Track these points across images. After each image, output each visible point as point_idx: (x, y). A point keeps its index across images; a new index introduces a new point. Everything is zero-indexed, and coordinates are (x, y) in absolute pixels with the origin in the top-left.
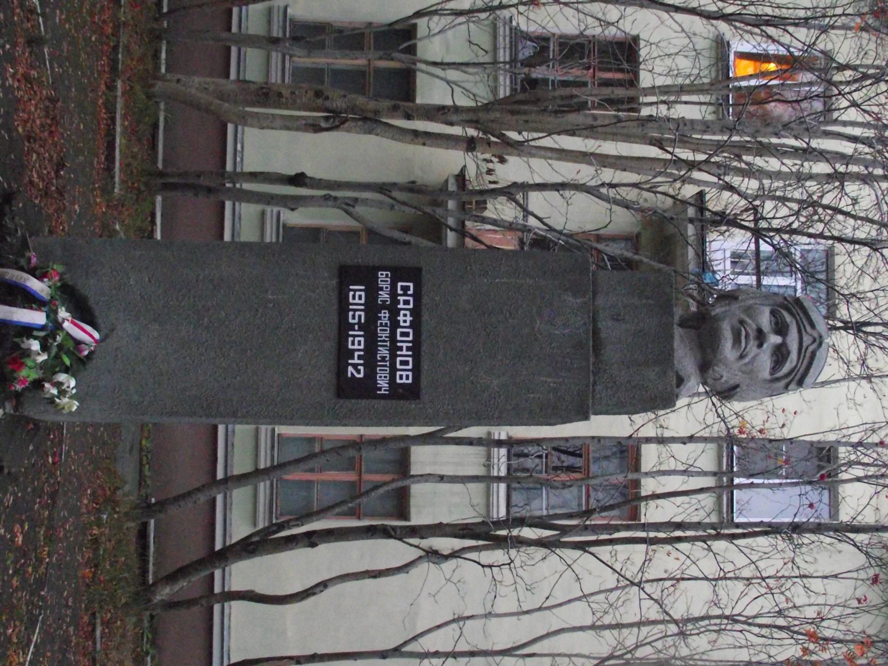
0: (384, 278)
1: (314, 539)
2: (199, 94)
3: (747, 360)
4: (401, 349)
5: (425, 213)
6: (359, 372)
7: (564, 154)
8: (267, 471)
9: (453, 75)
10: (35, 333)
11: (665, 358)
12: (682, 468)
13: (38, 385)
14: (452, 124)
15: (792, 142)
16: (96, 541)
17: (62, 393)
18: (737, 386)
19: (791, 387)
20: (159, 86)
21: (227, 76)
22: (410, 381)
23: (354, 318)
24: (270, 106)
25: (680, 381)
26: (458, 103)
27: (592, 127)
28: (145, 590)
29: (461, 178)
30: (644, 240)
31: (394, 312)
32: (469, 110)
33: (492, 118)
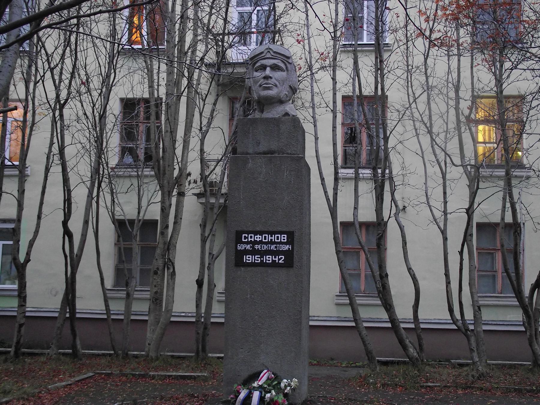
0: (240, 247)
1: (384, 275)
2: (156, 333)
3: (277, 83)
4: (271, 240)
6: (282, 258)
7: (186, 143)
8: (350, 299)
9: (144, 203)
10: (263, 396)
11: (276, 122)
13: (286, 395)
15: (177, 26)
16: (383, 385)
17: (289, 385)
18: (290, 86)
19: (290, 61)
20: (152, 354)
21: (147, 321)
22: (286, 236)
23: (258, 260)
24: (162, 298)
25: (287, 114)
26: (160, 199)
27: (171, 132)
28: (413, 362)
29: (199, 196)
30: (232, 95)
31: (255, 242)
32: (163, 194)
33: (167, 184)
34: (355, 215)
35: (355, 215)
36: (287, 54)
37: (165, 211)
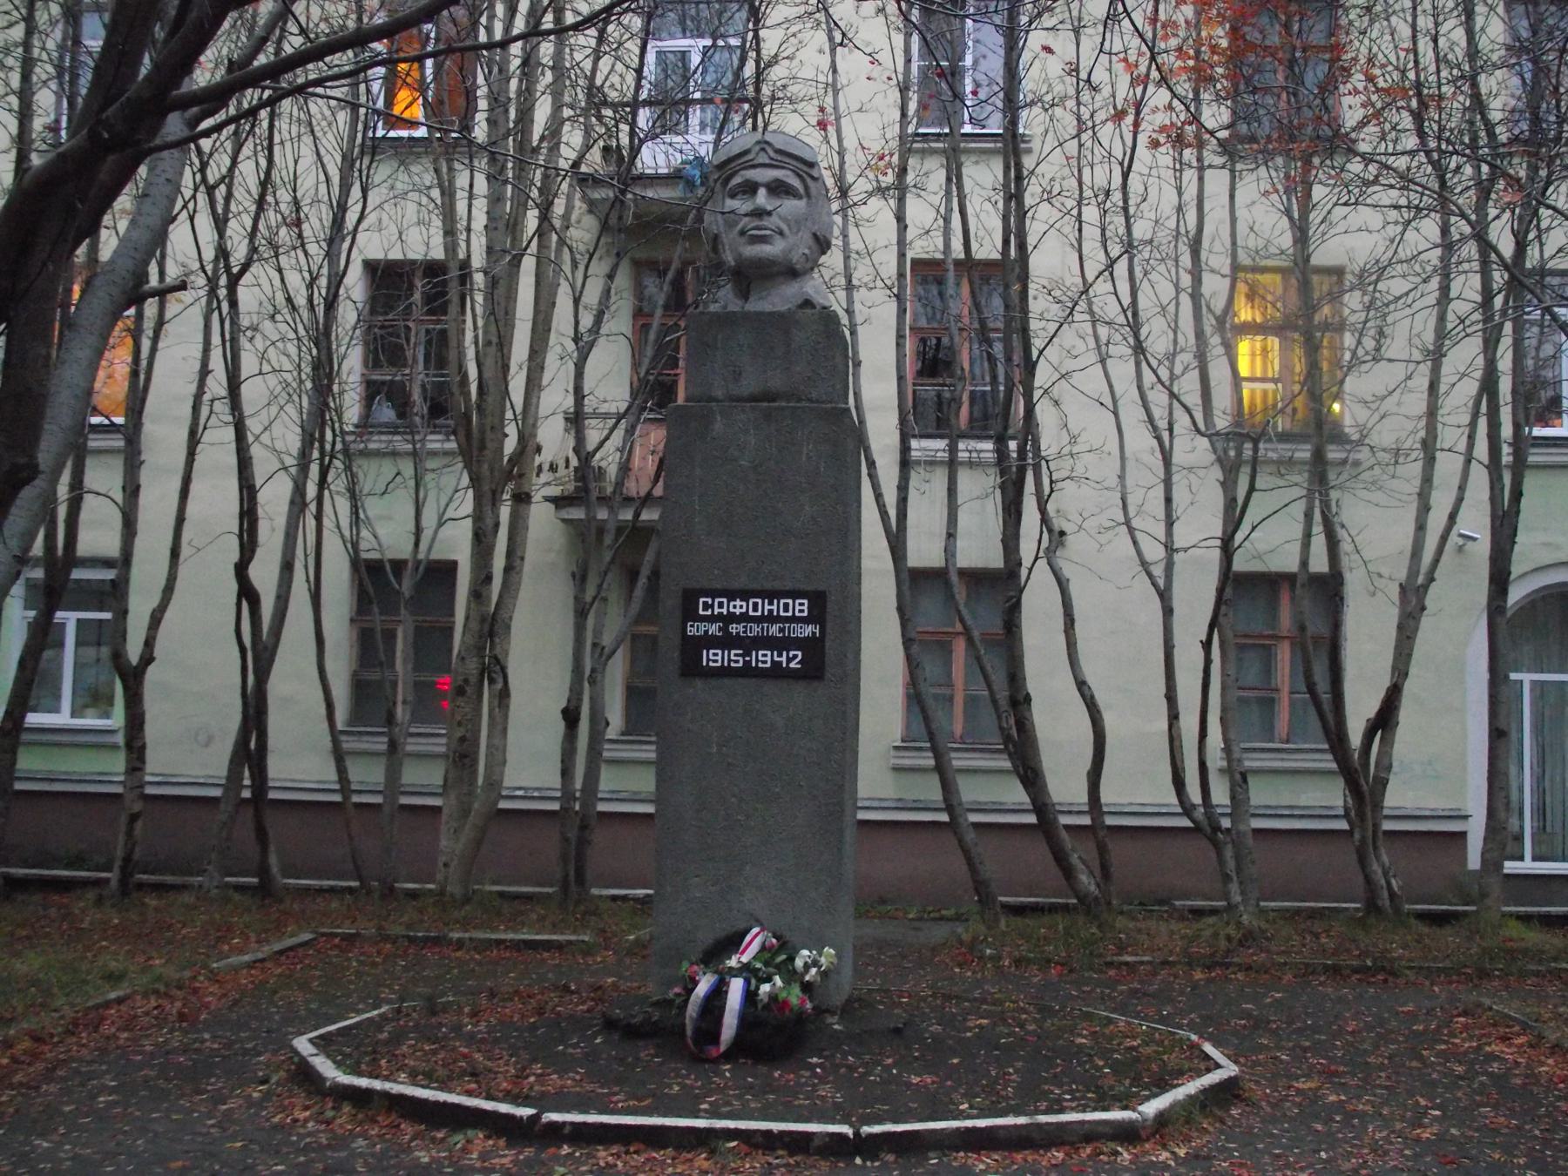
0: (693, 630)
1: (1021, 698)
2: (463, 840)
3: (784, 227)
4: (771, 611)
5: (612, 561)
6: (795, 656)
8: (938, 756)
10: (753, 987)
11: (781, 322)
12: (941, 222)
13: (807, 988)
14: (497, 525)
15: (514, 84)
16: (1018, 962)
17: (815, 963)
18: (815, 235)
19: (815, 173)
20: (454, 889)
21: (436, 810)
24: (477, 753)
25: (808, 303)
28: (1087, 906)
29: (559, 502)
30: (641, 254)
31: (732, 618)
32: (478, 499)
34: (949, 551)
35: (949, 551)
36: (807, 156)
37: (482, 540)
